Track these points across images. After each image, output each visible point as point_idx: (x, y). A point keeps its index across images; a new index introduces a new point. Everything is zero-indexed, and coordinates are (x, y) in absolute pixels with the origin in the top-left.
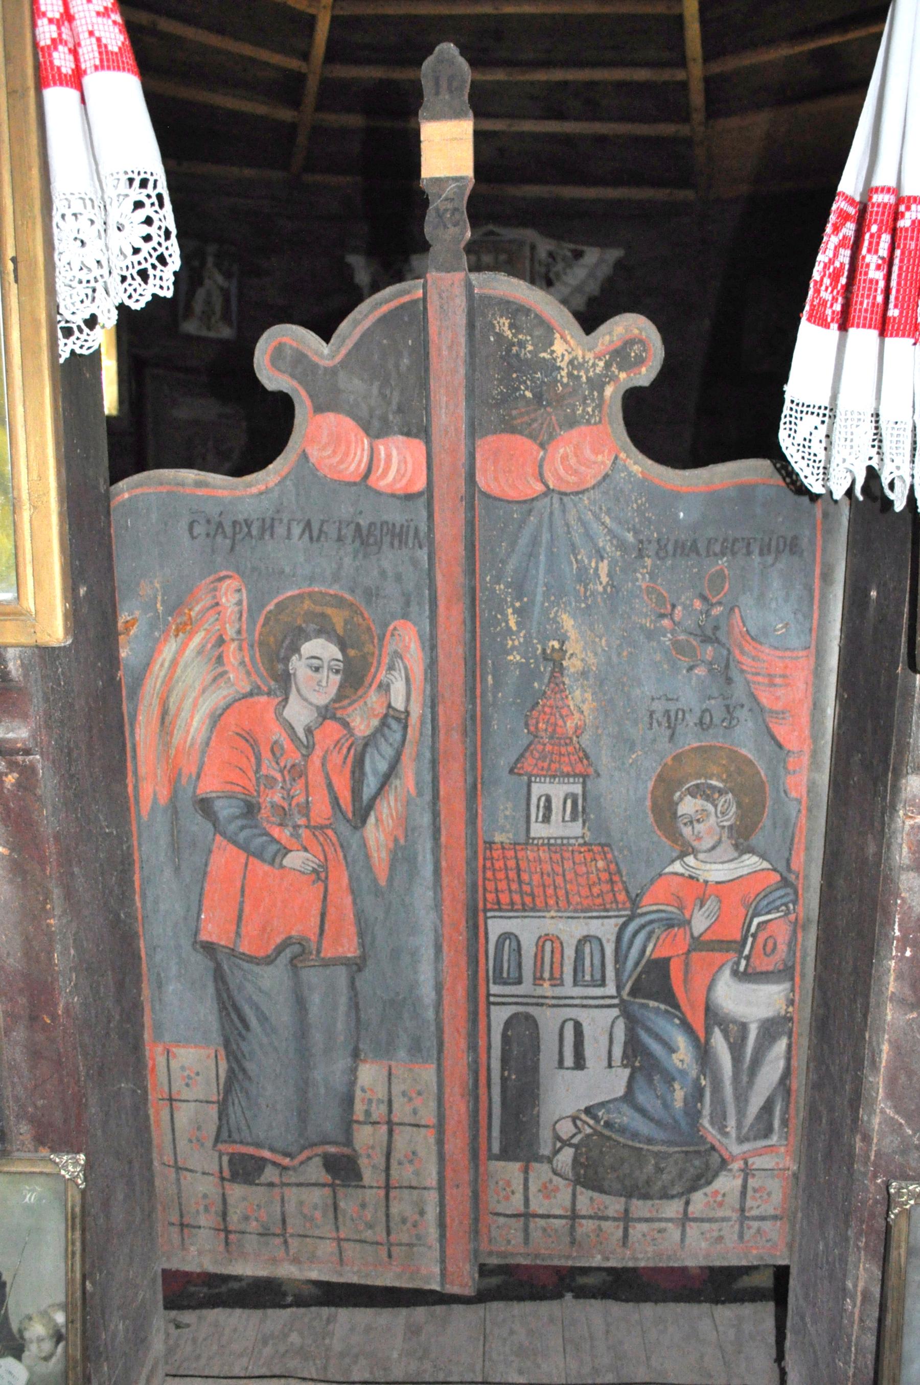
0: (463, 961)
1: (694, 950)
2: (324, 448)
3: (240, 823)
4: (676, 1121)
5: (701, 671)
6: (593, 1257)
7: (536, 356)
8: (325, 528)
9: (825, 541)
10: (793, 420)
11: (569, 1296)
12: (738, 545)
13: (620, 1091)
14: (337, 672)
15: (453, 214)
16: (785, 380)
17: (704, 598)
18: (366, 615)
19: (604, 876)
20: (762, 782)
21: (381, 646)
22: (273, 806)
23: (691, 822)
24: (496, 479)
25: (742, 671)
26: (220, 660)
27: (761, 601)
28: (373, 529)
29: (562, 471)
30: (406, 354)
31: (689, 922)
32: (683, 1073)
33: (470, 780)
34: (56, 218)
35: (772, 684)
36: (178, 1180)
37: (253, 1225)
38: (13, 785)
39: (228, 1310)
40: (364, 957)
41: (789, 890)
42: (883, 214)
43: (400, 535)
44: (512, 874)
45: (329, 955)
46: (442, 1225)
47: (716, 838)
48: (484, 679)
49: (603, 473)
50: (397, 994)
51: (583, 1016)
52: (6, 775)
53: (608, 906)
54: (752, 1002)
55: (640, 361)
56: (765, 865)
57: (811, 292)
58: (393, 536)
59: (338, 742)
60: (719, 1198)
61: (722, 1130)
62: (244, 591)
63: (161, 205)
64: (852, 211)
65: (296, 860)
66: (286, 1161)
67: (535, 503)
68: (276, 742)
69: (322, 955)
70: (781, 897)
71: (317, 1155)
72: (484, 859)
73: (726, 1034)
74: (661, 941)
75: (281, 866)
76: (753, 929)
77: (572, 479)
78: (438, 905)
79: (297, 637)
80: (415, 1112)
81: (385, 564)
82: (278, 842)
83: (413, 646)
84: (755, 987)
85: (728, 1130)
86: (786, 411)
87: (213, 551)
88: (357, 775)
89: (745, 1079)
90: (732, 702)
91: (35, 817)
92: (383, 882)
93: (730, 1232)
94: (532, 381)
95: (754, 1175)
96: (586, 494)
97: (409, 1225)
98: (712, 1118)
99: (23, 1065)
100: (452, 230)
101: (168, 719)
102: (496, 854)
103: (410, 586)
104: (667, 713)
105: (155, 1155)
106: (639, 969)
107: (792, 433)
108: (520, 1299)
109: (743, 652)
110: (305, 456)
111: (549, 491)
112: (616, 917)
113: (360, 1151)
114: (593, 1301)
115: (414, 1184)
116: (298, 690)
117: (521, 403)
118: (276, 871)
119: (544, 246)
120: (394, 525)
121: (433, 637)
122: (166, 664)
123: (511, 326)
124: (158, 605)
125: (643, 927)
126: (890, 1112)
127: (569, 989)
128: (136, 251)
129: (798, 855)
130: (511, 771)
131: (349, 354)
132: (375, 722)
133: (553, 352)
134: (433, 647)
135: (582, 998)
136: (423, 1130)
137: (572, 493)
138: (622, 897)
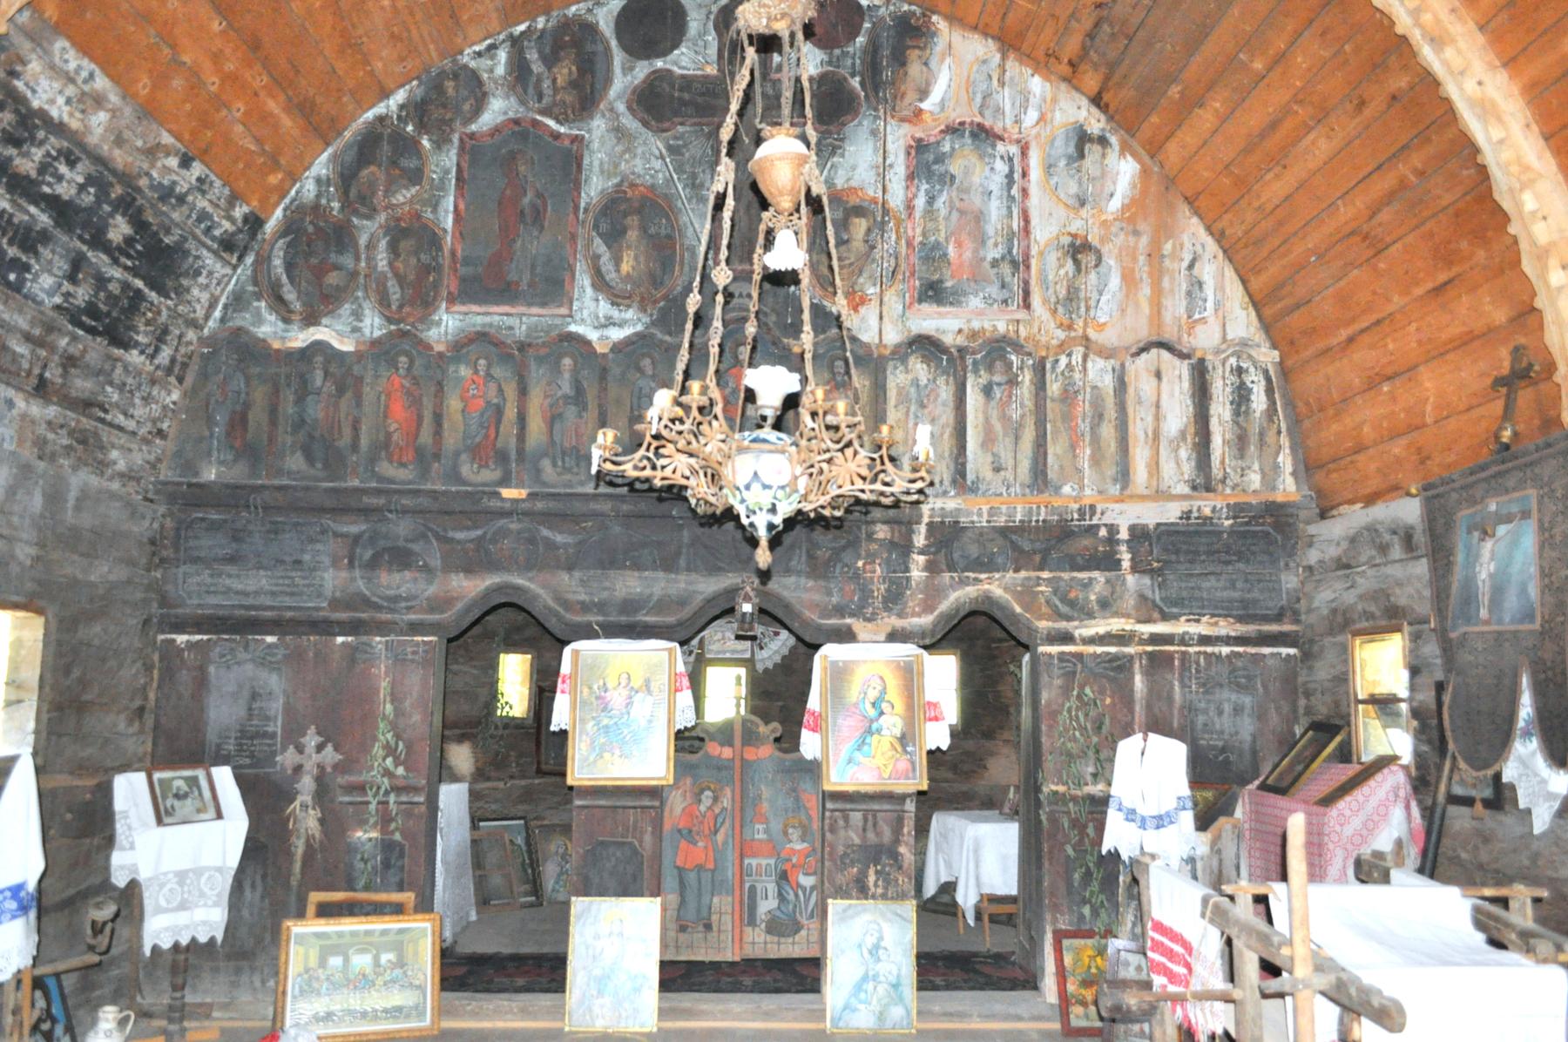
28: (720, 766)
54: (807, 881)
79: (702, 791)
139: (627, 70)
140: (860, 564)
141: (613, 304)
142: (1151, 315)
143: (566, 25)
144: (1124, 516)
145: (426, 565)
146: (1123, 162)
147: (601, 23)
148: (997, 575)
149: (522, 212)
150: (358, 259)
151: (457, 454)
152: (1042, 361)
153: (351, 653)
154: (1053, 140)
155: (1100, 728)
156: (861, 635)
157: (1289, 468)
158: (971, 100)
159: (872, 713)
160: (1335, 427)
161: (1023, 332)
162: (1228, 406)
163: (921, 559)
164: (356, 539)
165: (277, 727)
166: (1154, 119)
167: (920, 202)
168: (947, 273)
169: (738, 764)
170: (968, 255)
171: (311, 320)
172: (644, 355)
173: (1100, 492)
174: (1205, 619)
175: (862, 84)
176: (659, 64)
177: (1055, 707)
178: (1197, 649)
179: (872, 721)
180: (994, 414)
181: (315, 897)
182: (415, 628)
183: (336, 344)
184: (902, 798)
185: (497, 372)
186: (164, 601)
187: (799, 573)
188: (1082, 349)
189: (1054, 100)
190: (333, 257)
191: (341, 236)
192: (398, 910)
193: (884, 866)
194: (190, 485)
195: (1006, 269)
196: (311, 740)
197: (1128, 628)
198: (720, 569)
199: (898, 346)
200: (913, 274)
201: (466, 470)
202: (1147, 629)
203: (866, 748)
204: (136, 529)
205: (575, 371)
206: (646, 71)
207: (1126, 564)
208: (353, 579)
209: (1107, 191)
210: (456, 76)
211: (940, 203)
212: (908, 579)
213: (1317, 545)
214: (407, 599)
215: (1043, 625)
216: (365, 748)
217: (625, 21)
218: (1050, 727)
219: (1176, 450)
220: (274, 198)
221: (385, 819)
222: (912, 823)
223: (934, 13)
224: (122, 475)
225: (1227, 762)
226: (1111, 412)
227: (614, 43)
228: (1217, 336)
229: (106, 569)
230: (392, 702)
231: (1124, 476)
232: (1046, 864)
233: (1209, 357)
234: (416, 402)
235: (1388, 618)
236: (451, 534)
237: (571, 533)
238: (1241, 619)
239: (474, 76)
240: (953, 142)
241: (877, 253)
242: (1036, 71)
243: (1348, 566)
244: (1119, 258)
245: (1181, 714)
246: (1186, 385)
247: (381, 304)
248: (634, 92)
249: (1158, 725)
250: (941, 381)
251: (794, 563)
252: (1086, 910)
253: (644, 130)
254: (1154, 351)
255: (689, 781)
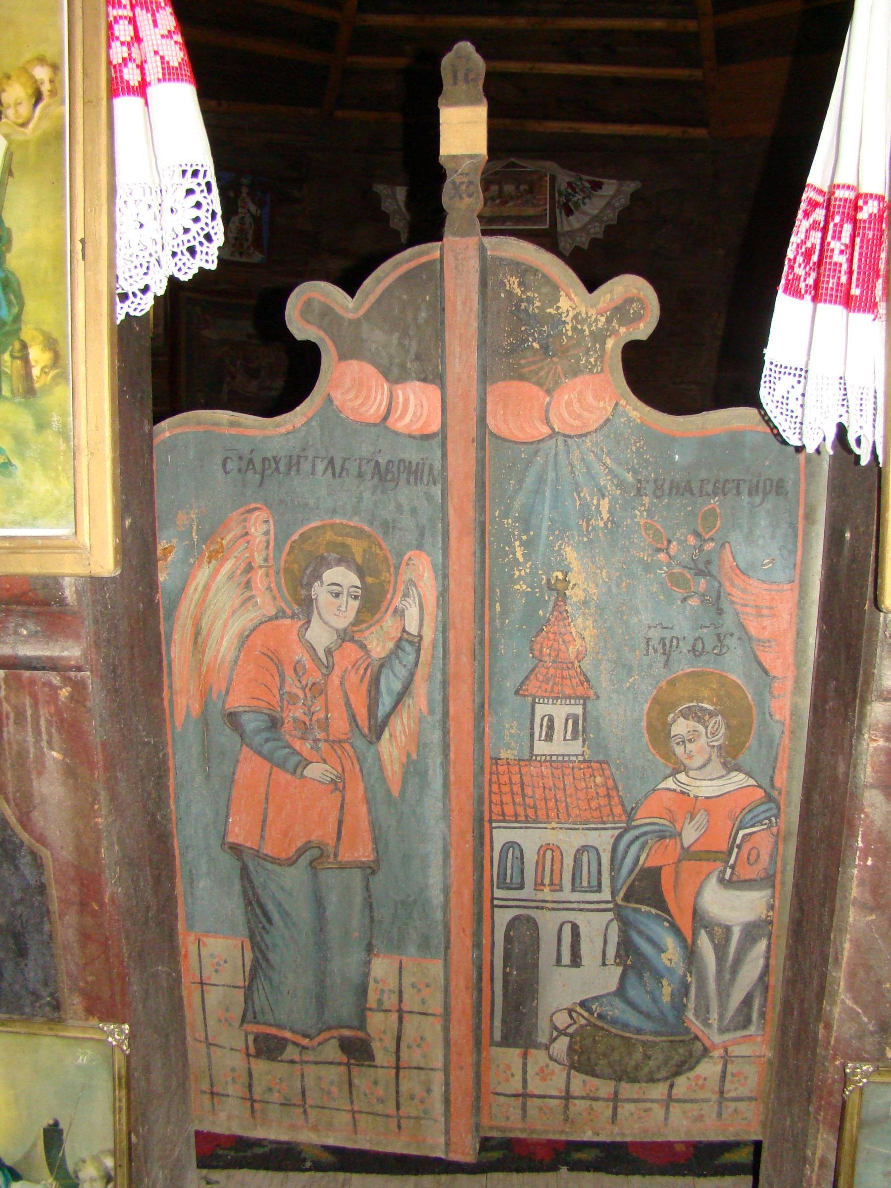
0: (469, 867)
1: (684, 859)
2: (347, 392)
3: (265, 735)
4: (662, 1012)
5: (694, 602)
6: (584, 1133)
7: (544, 311)
8: (347, 465)
9: (808, 484)
10: (772, 379)
11: (564, 1170)
12: (728, 486)
13: (613, 986)
14: (356, 597)
15: (468, 187)
16: (764, 344)
17: (697, 535)
18: (384, 544)
19: (602, 791)
20: (749, 704)
21: (397, 574)
22: (295, 720)
23: (683, 742)
24: (505, 421)
25: (732, 603)
26: (248, 585)
27: (750, 538)
29: (566, 415)
30: (423, 306)
31: (680, 835)
32: (671, 971)
33: (477, 700)
34: (119, 203)
35: (759, 615)
36: (209, 1055)
37: (275, 1097)
38: (66, 698)
39: (254, 1172)
40: (377, 861)
41: (773, 805)
42: (844, 207)
43: (416, 472)
44: (517, 789)
45: (346, 859)
46: (447, 1102)
47: (706, 757)
48: (492, 607)
49: (605, 418)
50: (409, 896)
51: (580, 919)
52: (61, 688)
53: (605, 819)
55: (638, 318)
56: (751, 782)
57: (786, 269)
58: (409, 472)
59: (356, 662)
60: (701, 1082)
61: (705, 1021)
62: (271, 522)
63: (209, 190)
64: (820, 199)
66: (306, 1042)
67: (541, 445)
68: (299, 662)
69: (339, 859)
70: (763, 812)
71: (335, 1038)
72: (491, 773)
73: (712, 939)
74: (653, 850)
75: (302, 776)
76: (738, 841)
77: (576, 423)
78: (446, 816)
79: (321, 564)
80: (423, 1002)
81: (403, 499)
82: (299, 754)
83: (426, 574)
84: (738, 893)
85: (710, 1022)
86: (766, 371)
87: (244, 486)
88: (373, 693)
89: (727, 976)
90: (723, 631)
91: (85, 728)
92: (396, 793)
93: (710, 1111)
94: (540, 334)
95: (733, 1062)
96: (589, 437)
97: (416, 1101)
98: (695, 1010)
99: (75, 945)
100: (467, 201)
101: (200, 640)
102: (501, 769)
103: (424, 521)
104: (663, 640)
105: (188, 1031)
106: (632, 877)
107: (771, 391)
108: (519, 1170)
109: (733, 585)
110: (329, 399)
111: (554, 434)
112: (613, 828)
113: (372, 1035)
114: (586, 1174)
115: (422, 1065)
116: (319, 614)
117: (529, 353)
118: (298, 781)
119: (564, 178)
120: (410, 462)
121: (445, 566)
122: (200, 588)
123: (520, 284)
124: (194, 534)
125: (637, 838)
126: (849, 1003)
127: (567, 894)
128: (186, 231)
129: (781, 773)
130: (517, 693)
131: (372, 307)
132: (390, 645)
133: (558, 308)
134: (445, 576)
135: (579, 902)
136: (430, 1018)
137: (576, 436)
138: (618, 810)
169: (461, 462)
255: (259, 526)
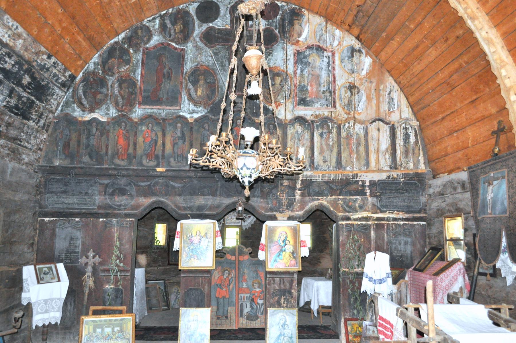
28: (231, 263)
54: (261, 302)
65: (224, 289)
79: (225, 271)
139: (200, 26)
140: (278, 194)
141: (195, 105)
142: (376, 111)
143: (179, 11)
144: (367, 178)
145: (131, 194)
146: (366, 58)
147: (191, 11)
148: (325, 198)
149: (164, 74)
150: (108, 90)
151: (141, 157)
152: (340, 125)
153: (105, 224)
154: (343, 51)
155: (360, 249)
156: (279, 218)
157: (423, 161)
158: (315, 37)
159: (283, 244)
160: (438, 147)
161: (333, 116)
162: (402, 140)
163: (299, 192)
164: (107, 185)
165: (79, 250)
166: (377, 44)
167: (299, 72)
168: (308, 95)
170: (315, 89)
171: (92, 111)
172: (205, 123)
173: (359, 169)
174: (395, 212)
175: (279, 32)
176: (211, 25)
177: (344, 242)
178: (392, 222)
179: (282, 247)
180: (324, 143)
181: (92, 308)
182: (127, 216)
183: (100, 119)
184: (293, 273)
185: (155, 128)
186: (40, 207)
187: (258, 197)
188: (353, 121)
189: (344, 38)
190: (100, 89)
191: (102, 82)
192: (120, 312)
193: (287, 297)
194: (50, 167)
195: (328, 94)
196: (91, 254)
197: (369, 215)
198: (231, 196)
199: (291, 120)
200: (296, 96)
201: (145, 162)
202: (375, 216)
203: (280, 256)
204: (31, 182)
205: (182, 128)
206: (206, 27)
207: (368, 194)
208: (106, 199)
209: (361, 68)
210: (141, 29)
211: (306, 72)
212: (295, 199)
213: (432, 187)
214: (123, 206)
215: (340, 214)
216: (110, 257)
217: (199, 10)
218: (343, 249)
219: (385, 155)
220: (79, 69)
221: (116, 281)
222: (296, 282)
223: (303, 8)
224: (26, 163)
225: (402, 261)
226: (363, 142)
227: (195, 18)
228: (399, 117)
229: (21, 195)
230: (119, 241)
231: (367, 164)
232: (342, 295)
233: (396, 124)
234: (127, 139)
235: (457, 212)
236: (139, 183)
237: (180, 183)
238: (407, 212)
239: (148, 28)
240: (309, 52)
241: (284, 89)
242: (337, 28)
243: (443, 195)
244: (365, 90)
245: (387, 245)
246: (388, 133)
247: (116, 105)
248: (202, 34)
249: (379, 248)
250: (306, 132)
251: (256, 193)
252: (355, 311)
253: (205, 47)
254: (377, 122)
255: (220, 268)
